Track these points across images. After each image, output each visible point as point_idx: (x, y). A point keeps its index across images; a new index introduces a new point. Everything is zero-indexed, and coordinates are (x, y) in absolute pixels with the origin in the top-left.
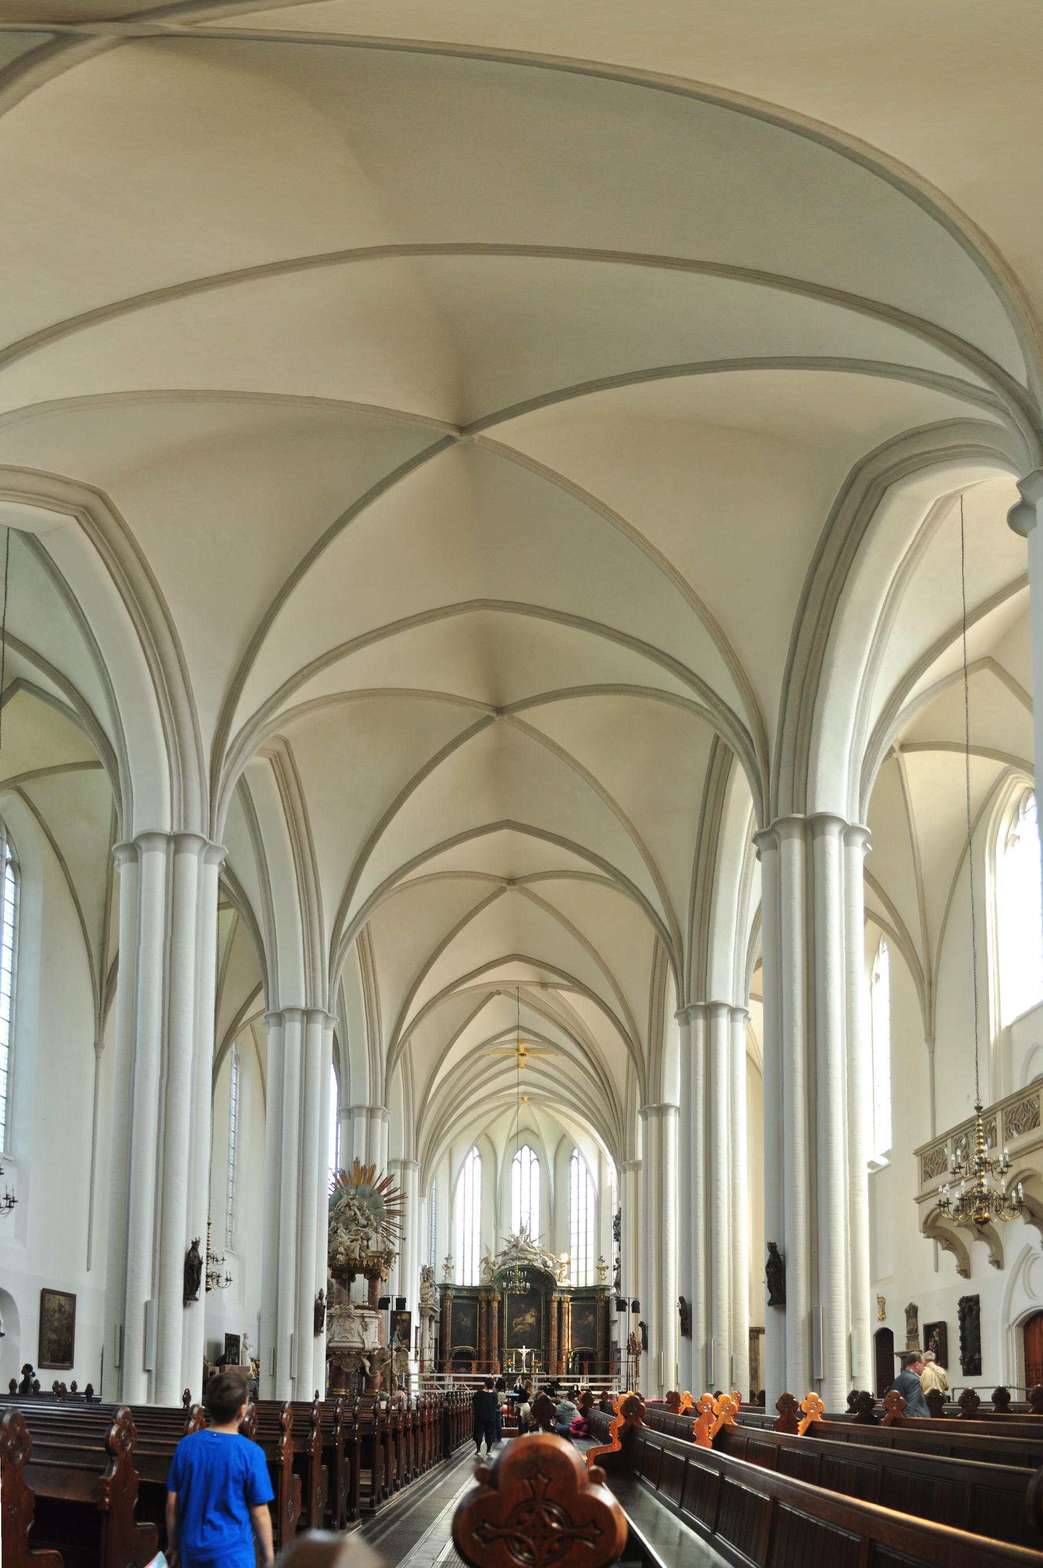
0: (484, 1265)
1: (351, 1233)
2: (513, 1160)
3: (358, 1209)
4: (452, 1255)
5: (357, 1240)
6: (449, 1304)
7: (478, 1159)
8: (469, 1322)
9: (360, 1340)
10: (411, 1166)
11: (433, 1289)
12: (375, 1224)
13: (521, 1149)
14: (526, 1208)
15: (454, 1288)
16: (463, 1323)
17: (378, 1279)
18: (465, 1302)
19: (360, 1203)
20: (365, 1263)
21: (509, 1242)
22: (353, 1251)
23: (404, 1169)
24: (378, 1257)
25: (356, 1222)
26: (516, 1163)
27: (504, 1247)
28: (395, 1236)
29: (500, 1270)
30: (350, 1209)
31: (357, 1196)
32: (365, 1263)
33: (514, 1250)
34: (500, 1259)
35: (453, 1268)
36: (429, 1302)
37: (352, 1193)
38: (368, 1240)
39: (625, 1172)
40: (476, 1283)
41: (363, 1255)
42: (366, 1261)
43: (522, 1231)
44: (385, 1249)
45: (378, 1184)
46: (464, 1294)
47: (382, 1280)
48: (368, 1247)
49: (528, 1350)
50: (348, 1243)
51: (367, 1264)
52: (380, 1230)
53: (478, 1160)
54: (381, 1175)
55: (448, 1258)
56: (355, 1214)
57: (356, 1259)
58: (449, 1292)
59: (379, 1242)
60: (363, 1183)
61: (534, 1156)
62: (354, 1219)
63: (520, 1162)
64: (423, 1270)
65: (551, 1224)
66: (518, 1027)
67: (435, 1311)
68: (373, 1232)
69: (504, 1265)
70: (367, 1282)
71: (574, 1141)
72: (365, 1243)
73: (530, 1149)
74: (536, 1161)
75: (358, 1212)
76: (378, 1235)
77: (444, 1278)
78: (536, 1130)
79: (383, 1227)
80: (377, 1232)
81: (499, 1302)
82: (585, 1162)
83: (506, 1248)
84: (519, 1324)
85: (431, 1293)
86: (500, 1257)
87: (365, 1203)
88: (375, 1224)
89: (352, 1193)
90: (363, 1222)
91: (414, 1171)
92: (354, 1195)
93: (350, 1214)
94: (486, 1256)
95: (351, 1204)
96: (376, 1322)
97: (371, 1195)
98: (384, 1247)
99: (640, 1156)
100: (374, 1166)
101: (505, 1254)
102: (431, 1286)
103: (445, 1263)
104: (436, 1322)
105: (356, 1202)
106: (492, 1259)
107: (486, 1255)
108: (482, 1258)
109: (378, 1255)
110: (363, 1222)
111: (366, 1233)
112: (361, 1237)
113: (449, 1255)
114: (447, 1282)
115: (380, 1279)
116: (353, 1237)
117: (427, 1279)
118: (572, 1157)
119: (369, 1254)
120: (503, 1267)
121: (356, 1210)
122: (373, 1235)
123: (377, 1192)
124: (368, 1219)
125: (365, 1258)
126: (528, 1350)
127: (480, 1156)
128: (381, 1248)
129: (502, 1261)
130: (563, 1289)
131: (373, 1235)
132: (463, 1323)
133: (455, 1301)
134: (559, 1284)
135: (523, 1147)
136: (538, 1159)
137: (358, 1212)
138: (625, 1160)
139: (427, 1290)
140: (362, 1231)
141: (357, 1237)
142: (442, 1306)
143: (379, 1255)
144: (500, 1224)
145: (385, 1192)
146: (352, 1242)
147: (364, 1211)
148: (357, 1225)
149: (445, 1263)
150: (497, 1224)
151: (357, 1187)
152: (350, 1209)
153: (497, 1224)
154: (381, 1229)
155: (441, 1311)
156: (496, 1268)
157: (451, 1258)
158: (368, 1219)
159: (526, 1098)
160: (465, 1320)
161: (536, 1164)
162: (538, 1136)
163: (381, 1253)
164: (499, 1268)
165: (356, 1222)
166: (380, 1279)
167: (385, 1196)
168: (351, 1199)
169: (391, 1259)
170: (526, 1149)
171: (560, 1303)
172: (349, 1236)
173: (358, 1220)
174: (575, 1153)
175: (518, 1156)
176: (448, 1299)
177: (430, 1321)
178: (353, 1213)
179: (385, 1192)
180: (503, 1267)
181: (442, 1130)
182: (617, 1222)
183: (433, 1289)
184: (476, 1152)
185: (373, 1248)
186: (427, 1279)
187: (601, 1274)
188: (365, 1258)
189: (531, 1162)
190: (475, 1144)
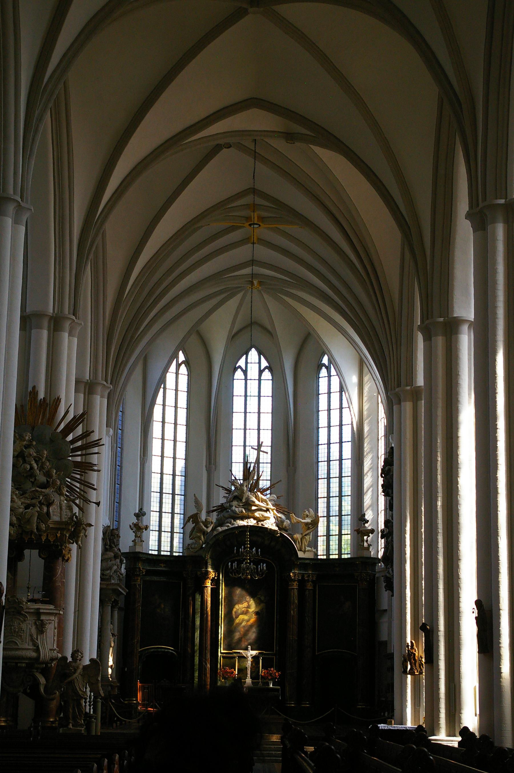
0: (191, 525)
1: (25, 495)
2: (235, 369)
3: (36, 462)
4: (145, 510)
5: (34, 506)
6: (139, 581)
7: (183, 365)
8: (167, 610)
9: (31, 647)
10: (99, 389)
11: (118, 560)
12: (58, 482)
13: (247, 353)
14: (252, 440)
15: (147, 559)
16: (158, 610)
17: (58, 559)
18: (162, 579)
19: (37, 452)
20: (44, 538)
21: (229, 491)
22: (29, 521)
23: (89, 394)
24: (62, 530)
25: (32, 480)
26: (239, 370)
27: (220, 498)
28: (87, 501)
29: (215, 533)
30: (25, 461)
31: (34, 443)
32: (44, 538)
33: (235, 503)
34: (214, 517)
35: (146, 529)
36: (113, 581)
37: (27, 438)
38: (49, 504)
39: (399, 403)
40: (178, 549)
41: (43, 526)
42: (45, 534)
43: (247, 473)
44: (71, 518)
45: (62, 426)
46: (162, 568)
47: (63, 559)
48: (48, 514)
49: (254, 653)
50: (21, 510)
51: (47, 540)
52: (65, 491)
53: (183, 368)
54: (67, 412)
55: (141, 514)
56: (32, 468)
57: (32, 532)
58: (140, 565)
59: (64, 508)
60: (42, 423)
61: (264, 363)
62: (31, 474)
63: (245, 372)
64: (104, 534)
65: (288, 465)
66: (253, 191)
67: (120, 594)
68: (55, 494)
69: (221, 525)
70: (42, 562)
71: (324, 344)
72: (45, 509)
73: (260, 353)
74: (267, 370)
75: (35, 466)
76: (62, 498)
77: (131, 544)
78: (269, 327)
79: (68, 486)
80: (61, 494)
81: (213, 580)
82: (339, 374)
83: (223, 501)
84: (243, 613)
85: (115, 567)
86: (215, 514)
87: (46, 452)
88: (58, 482)
89: (27, 438)
90: (42, 479)
91: (102, 397)
92: (30, 441)
93: (25, 469)
94: (195, 511)
95: (26, 454)
96: (55, 620)
97: (52, 441)
98: (69, 514)
99: (420, 381)
100: (58, 400)
101: (222, 508)
102: (116, 557)
103: (135, 520)
104: (120, 609)
105: (32, 451)
106: (203, 516)
107: (193, 511)
108: (189, 514)
109: (61, 526)
110: (42, 479)
111: (46, 496)
112: (40, 502)
113: (141, 509)
114: (138, 549)
115: (61, 559)
116: (28, 502)
117: (110, 546)
118: (320, 366)
119: (51, 526)
120: (220, 529)
121: (33, 462)
122: (56, 499)
123: (61, 436)
124: (48, 475)
125: (45, 532)
126: (254, 653)
127: (186, 363)
128: (66, 515)
129: (217, 520)
130: (307, 561)
131: (56, 499)
132: (158, 610)
133: (148, 578)
134: (300, 555)
135: (250, 349)
136: (269, 368)
137: (35, 466)
138: (399, 385)
139: (110, 563)
140: (42, 492)
141: (34, 501)
142: (128, 585)
143: (64, 526)
144: (215, 464)
145: (70, 438)
146: (27, 507)
147: (43, 464)
148: (33, 483)
149: (135, 520)
150: (210, 463)
151: (33, 429)
152: (25, 461)
153: (210, 463)
154: (65, 489)
155: (128, 595)
156: (209, 529)
157: (144, 514)
158: (48, 475)
159: (255, 282)
160: (163, 606)
161: (266, 374)
162: (272, 335)
163: (67, 524)
164: (213, 529)
165: (32, 480)
166: (61, 559)
167: (73, 441)
168: (27, 447)
169: (80, 531)
170: (253, 354)
171: (302, 583)
172: (23, 500)
173: (35, 476)
174: (325, 360)
175: (242, 362)
176: (139, 575)
177: (113, 608)
178: (28, 467)
179: (70, 438)
180: (220, 529)
181: (137, 329)
182: (387, 469)
183: (118, 560)
184: (182, 357)
185: (55, 518)
186: (110, 546)
187: (363, 541)
188: (45, 532)
189: (261, 372)
190: (182, 346)
